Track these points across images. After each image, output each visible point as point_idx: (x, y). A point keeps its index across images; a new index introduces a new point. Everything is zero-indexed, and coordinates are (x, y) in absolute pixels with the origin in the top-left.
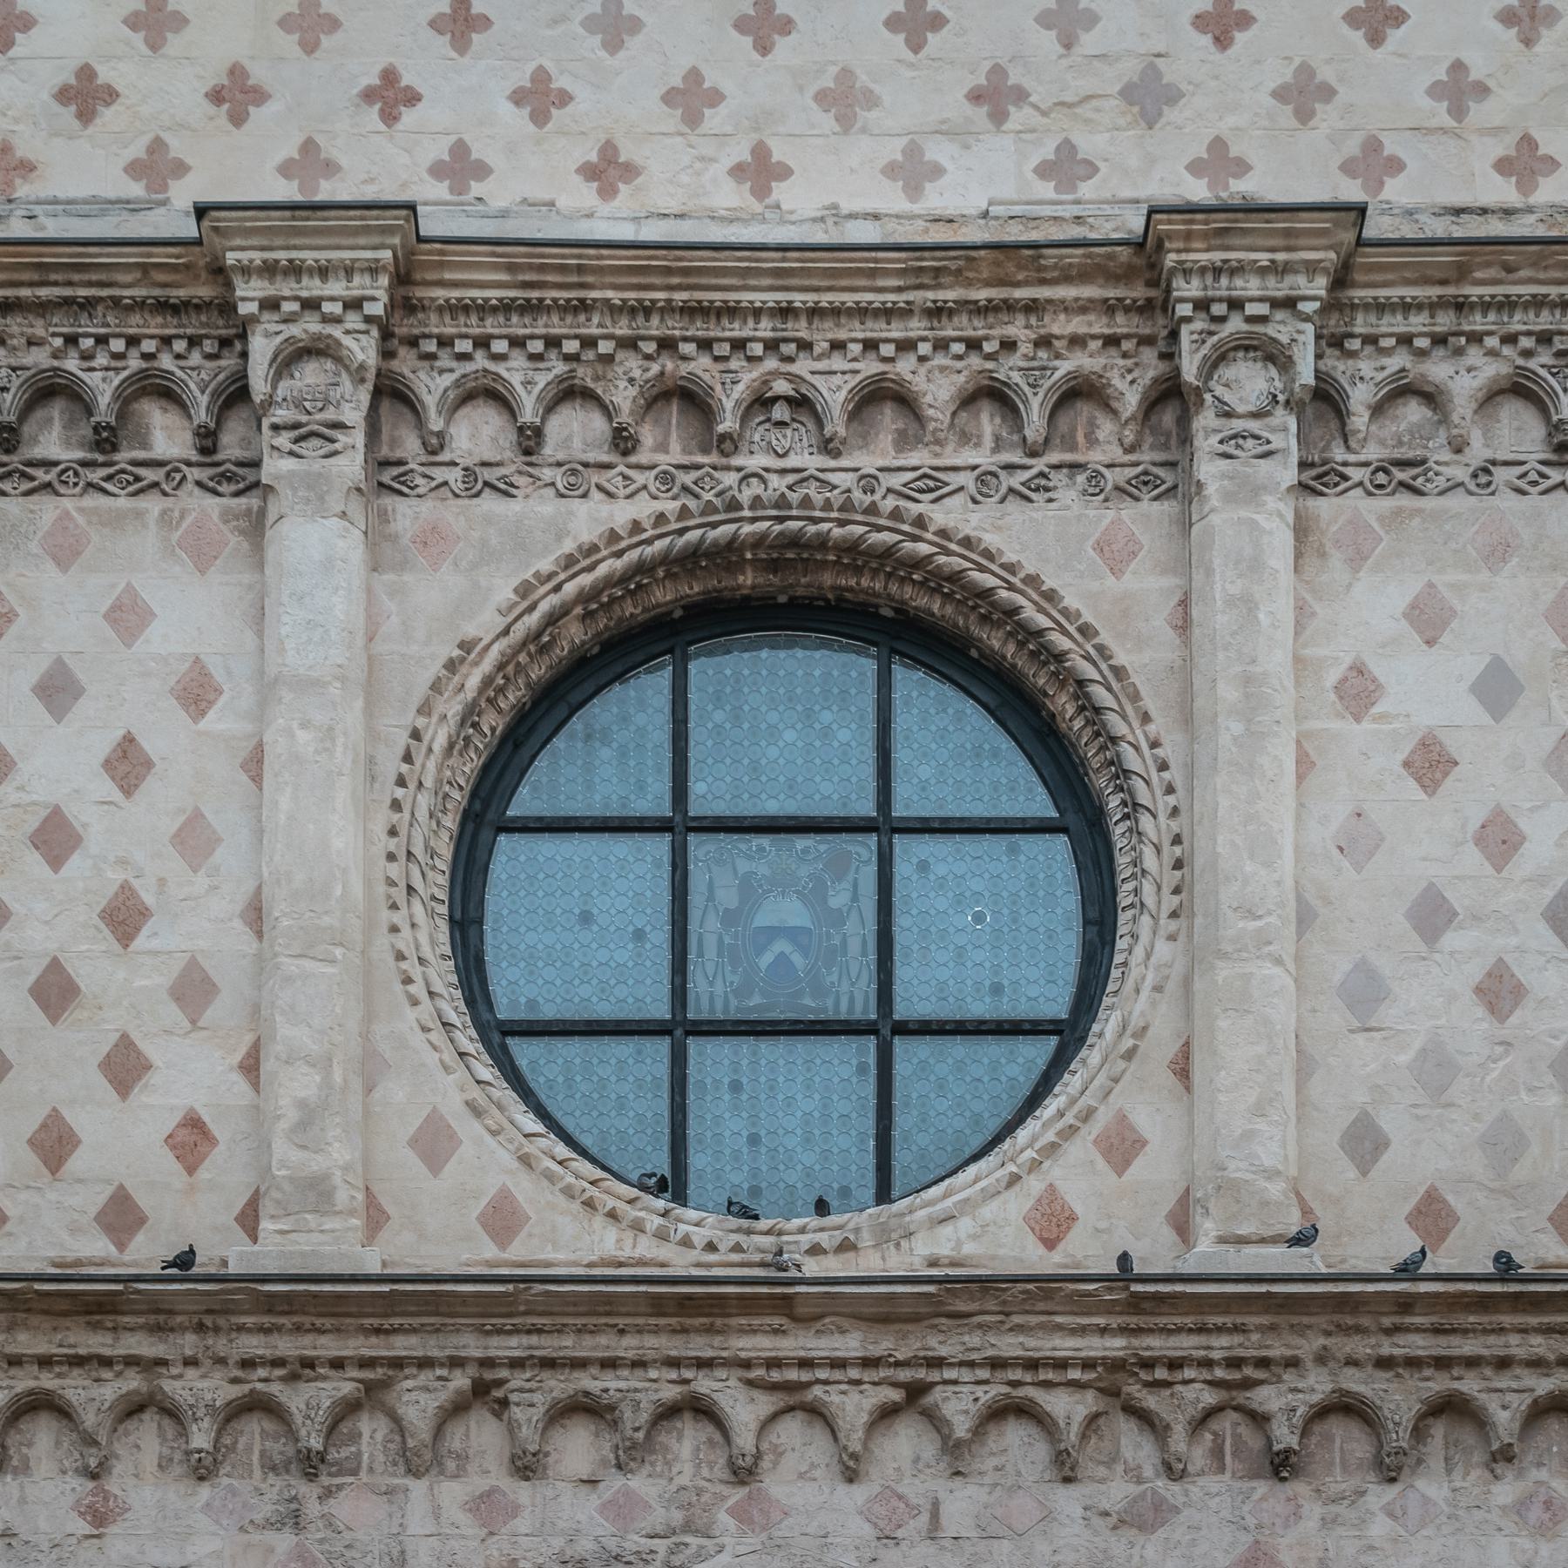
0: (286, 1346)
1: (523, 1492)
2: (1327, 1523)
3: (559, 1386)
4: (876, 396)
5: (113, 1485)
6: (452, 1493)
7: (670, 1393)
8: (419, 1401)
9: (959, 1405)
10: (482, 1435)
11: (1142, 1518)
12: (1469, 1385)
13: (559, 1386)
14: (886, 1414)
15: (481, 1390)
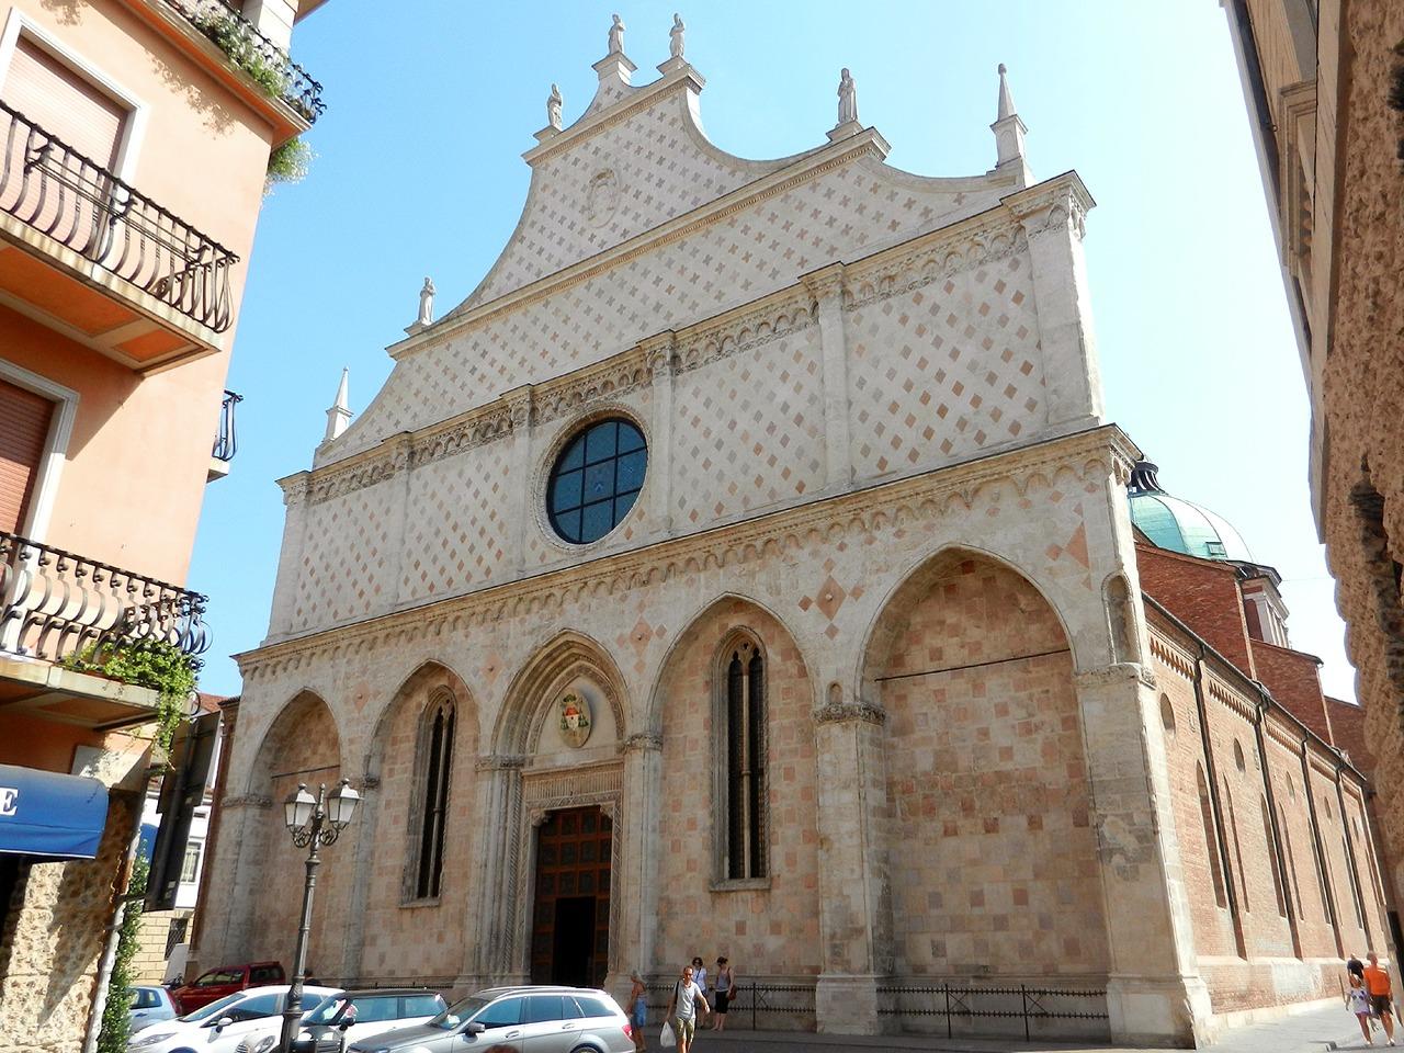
0: (491, 599)
1: (527, 617)
2: (654, 593)
3: (531, 596)
4: (605, 385)
5: (469, 629)
6: (517, 619)
7: (547, 593)
8: (511, 603)
9: (592, 583)
10: (522, 607)
11: (624, 599)
12: (674, 560)
13: (531, 596)
14: (582, 588)
15: (520, 599)
